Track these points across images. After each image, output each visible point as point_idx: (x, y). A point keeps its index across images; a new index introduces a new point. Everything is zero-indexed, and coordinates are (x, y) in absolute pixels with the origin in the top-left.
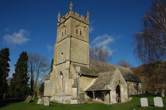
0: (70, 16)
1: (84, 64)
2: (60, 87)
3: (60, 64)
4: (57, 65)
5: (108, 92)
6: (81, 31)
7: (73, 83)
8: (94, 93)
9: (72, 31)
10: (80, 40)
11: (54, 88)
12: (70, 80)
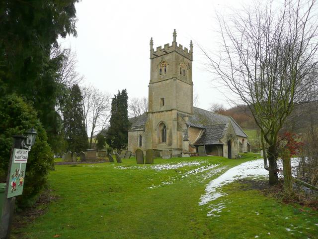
1: (188, 113)
3: (159, 112)
5: (222, 146)
7: (183, 136)
12: (179, 132)
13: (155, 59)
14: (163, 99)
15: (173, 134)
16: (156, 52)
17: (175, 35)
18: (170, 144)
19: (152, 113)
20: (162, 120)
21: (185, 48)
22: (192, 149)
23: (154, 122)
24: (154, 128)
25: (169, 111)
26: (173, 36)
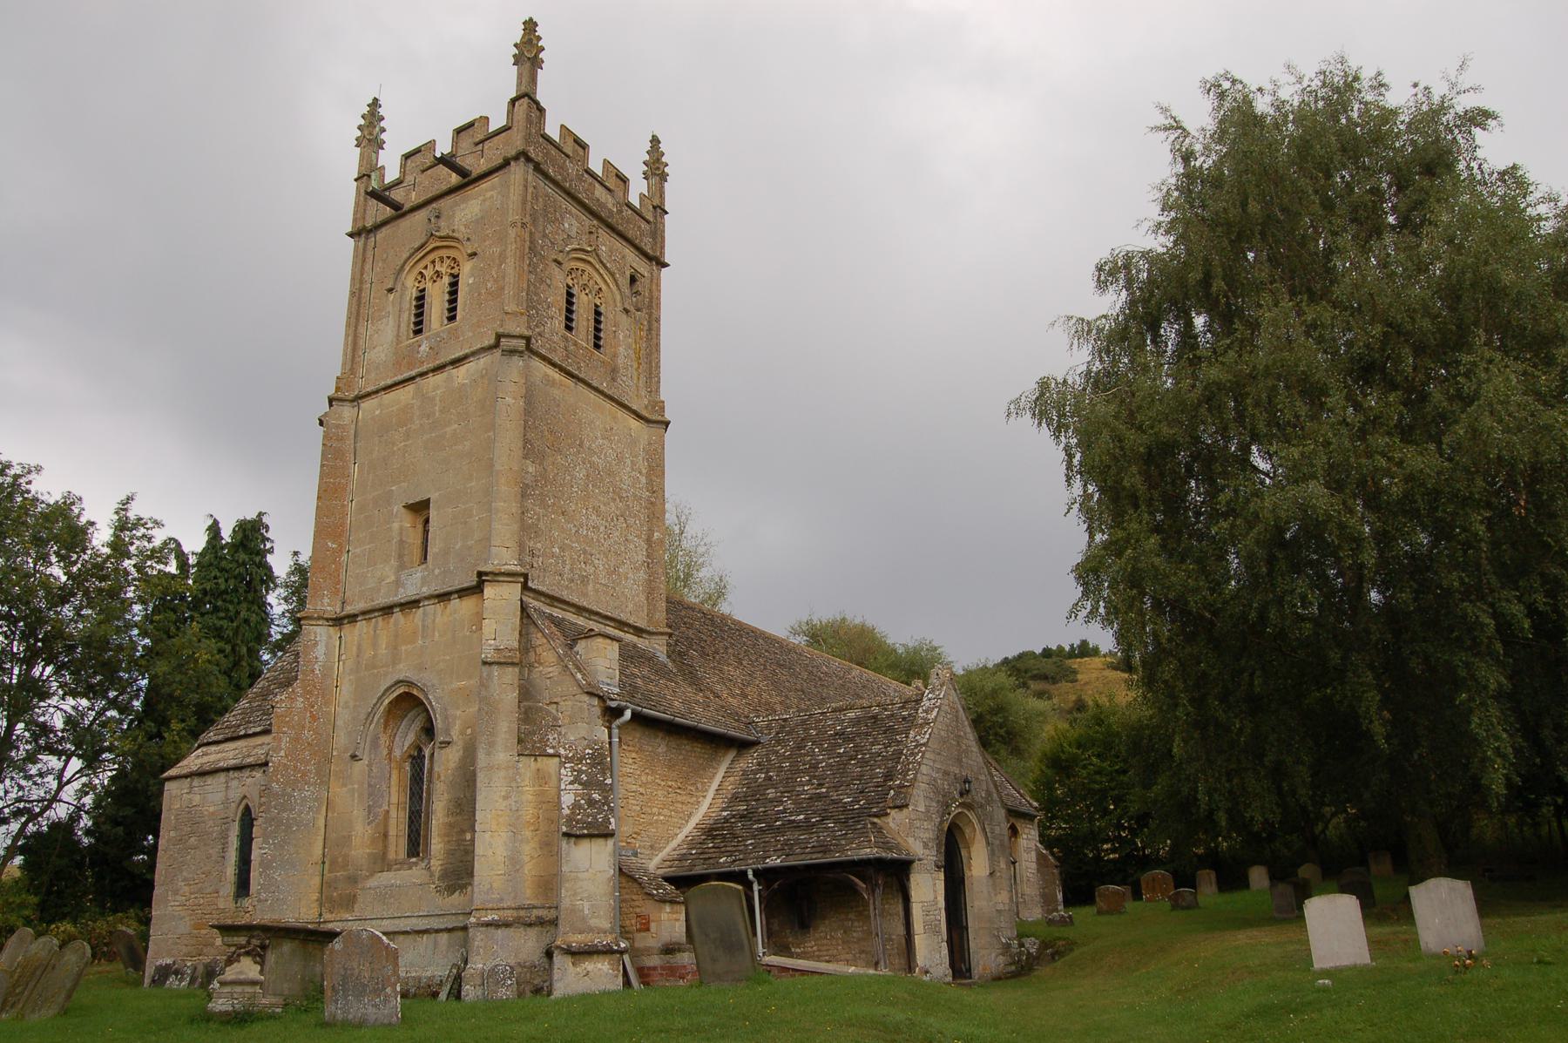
0: (523, 155)
2: (385, 847)
4: (352, 618)
5: (896, 872)
6: (598, 313)
7: (567, 799)
8: (756, 887)
9: (532, 305)
10: (592, 395)
11: (318, 850)
12: (529, 766)
13: (382, 234)
14: (420, 508)
15: (481, 778)
16: (397, 183)
17: (529, 53)
18: (459, 874)
19: (338, 621)
20: (404, 671)
21: (607, 163)
22: (648, 908)
23: (346, 691)
24: (341, 740)
25: (463, 593)
26: (518, 60)
